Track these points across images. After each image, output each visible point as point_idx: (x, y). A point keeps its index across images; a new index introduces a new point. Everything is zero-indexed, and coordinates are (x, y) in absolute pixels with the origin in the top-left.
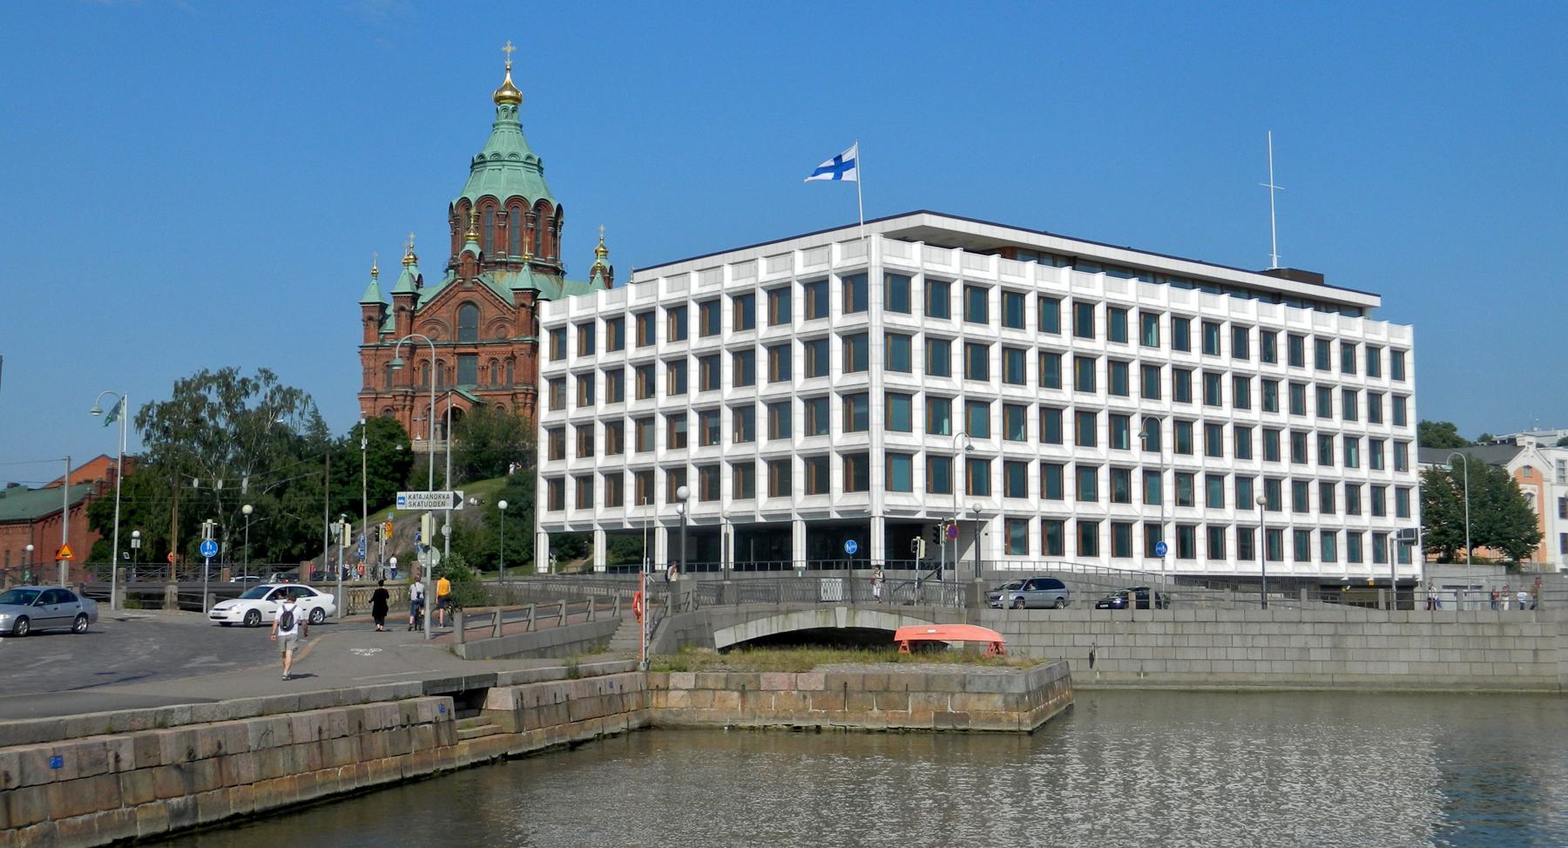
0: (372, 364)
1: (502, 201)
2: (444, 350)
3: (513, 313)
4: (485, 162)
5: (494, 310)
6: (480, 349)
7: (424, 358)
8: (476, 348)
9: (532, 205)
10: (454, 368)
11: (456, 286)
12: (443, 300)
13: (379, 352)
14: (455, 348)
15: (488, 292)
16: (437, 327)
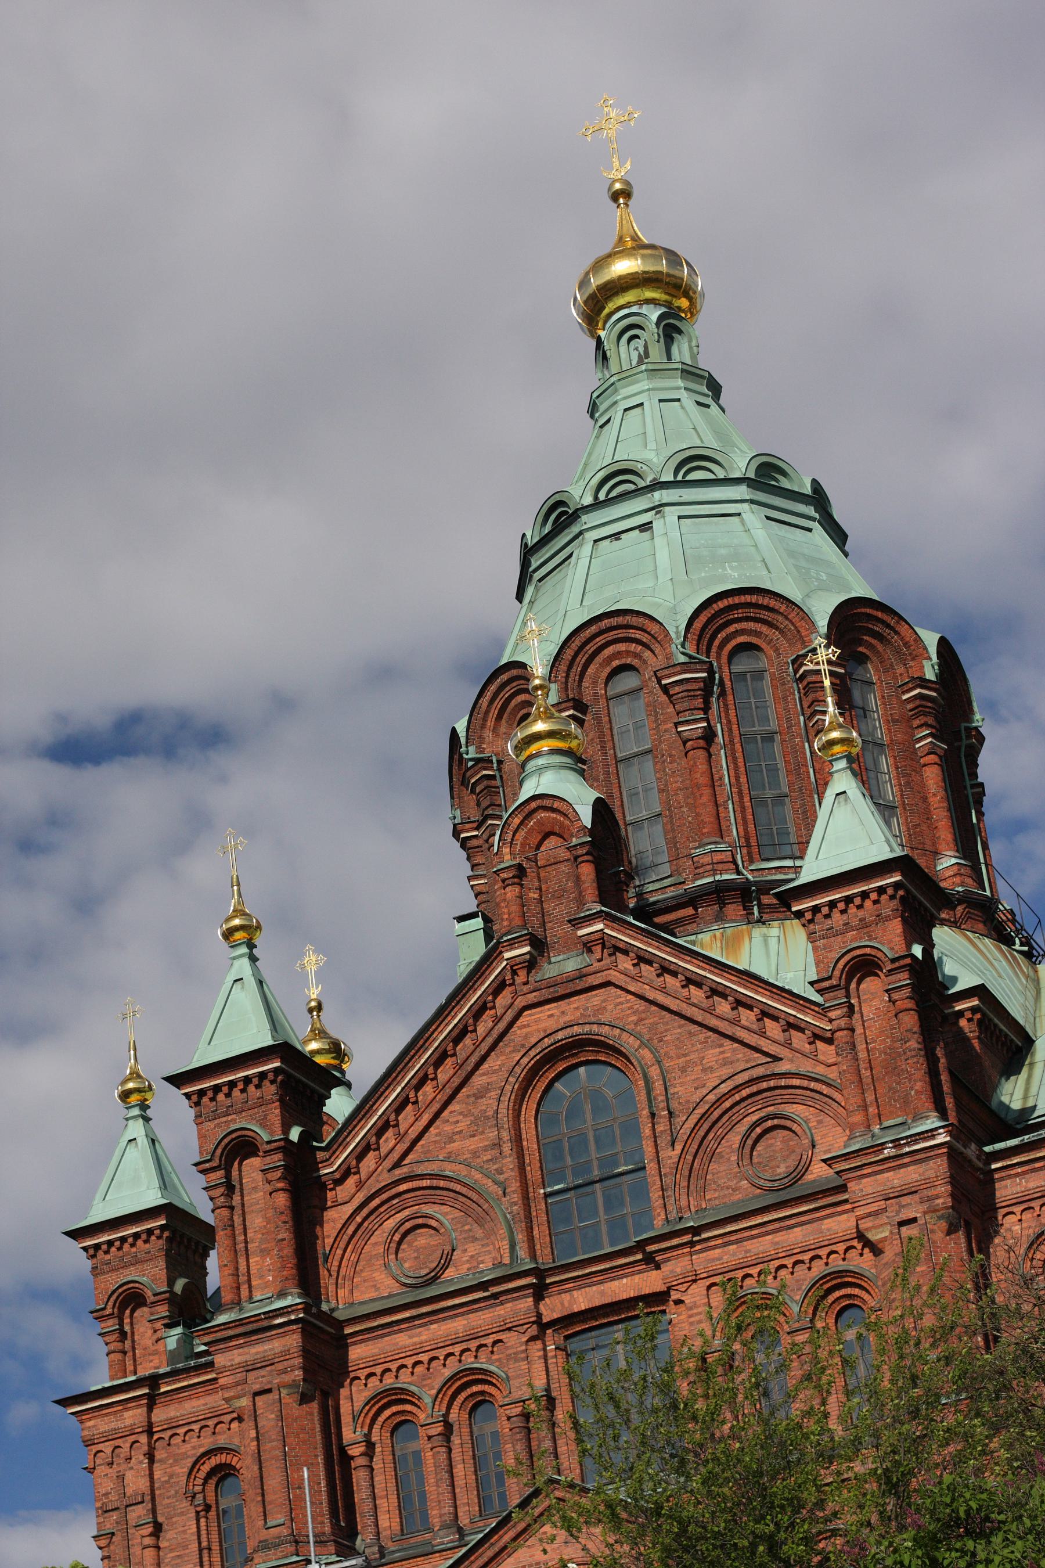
0: (136, 1482)
1: (676, 624)
2: (483, 1319)
3: (816, 1037)
4: (575, 516)
5: (712, 1055)
6: (676, 1267)
7: (389, 1380)
8: (651, 1261)
9: (822, 623)
10: (551, 1402)
11: (499, 987)
12: (444, 1073)
13: (159, 1415)
14: (539, 1292)
15: (665, 969)
16: (442, 1214)
